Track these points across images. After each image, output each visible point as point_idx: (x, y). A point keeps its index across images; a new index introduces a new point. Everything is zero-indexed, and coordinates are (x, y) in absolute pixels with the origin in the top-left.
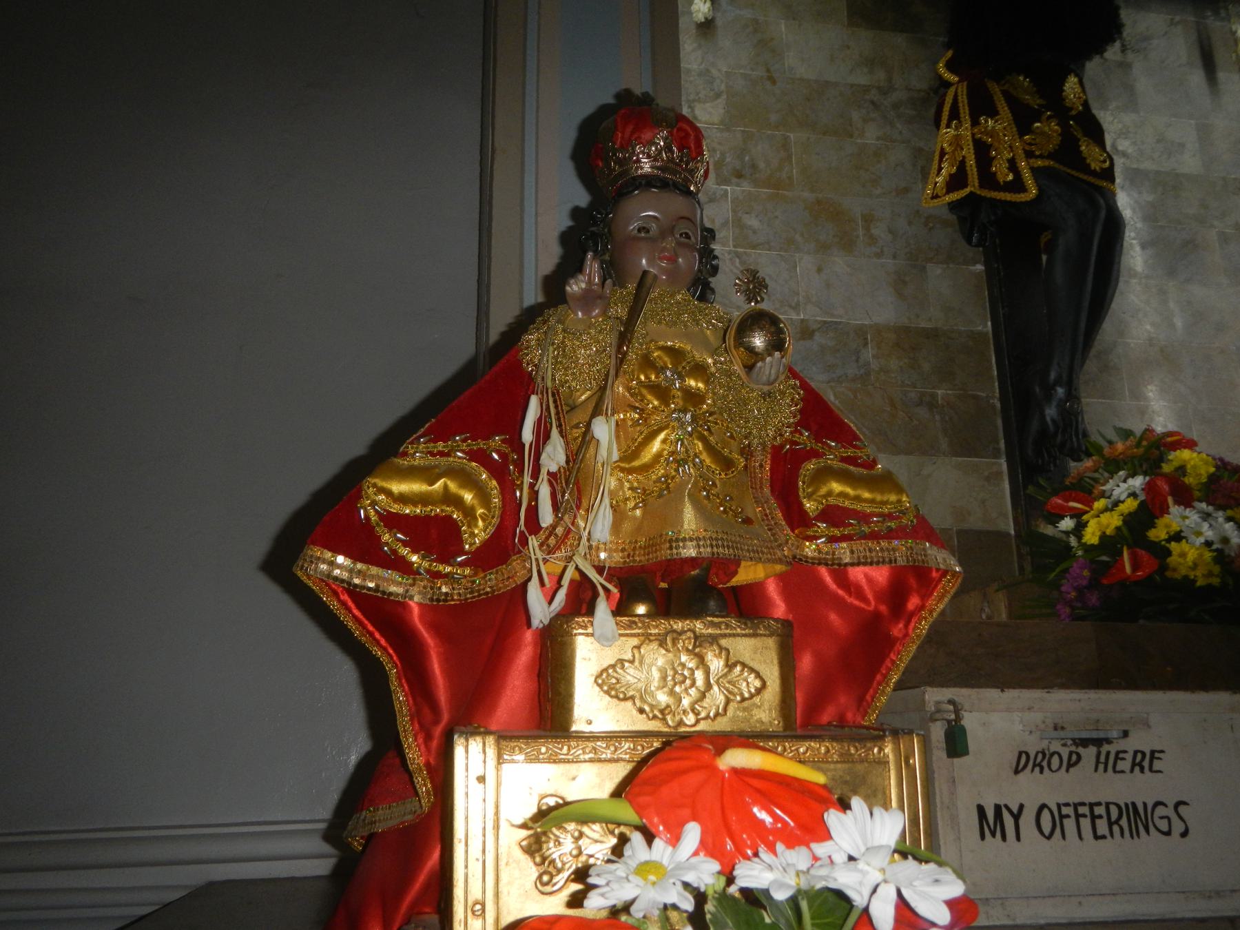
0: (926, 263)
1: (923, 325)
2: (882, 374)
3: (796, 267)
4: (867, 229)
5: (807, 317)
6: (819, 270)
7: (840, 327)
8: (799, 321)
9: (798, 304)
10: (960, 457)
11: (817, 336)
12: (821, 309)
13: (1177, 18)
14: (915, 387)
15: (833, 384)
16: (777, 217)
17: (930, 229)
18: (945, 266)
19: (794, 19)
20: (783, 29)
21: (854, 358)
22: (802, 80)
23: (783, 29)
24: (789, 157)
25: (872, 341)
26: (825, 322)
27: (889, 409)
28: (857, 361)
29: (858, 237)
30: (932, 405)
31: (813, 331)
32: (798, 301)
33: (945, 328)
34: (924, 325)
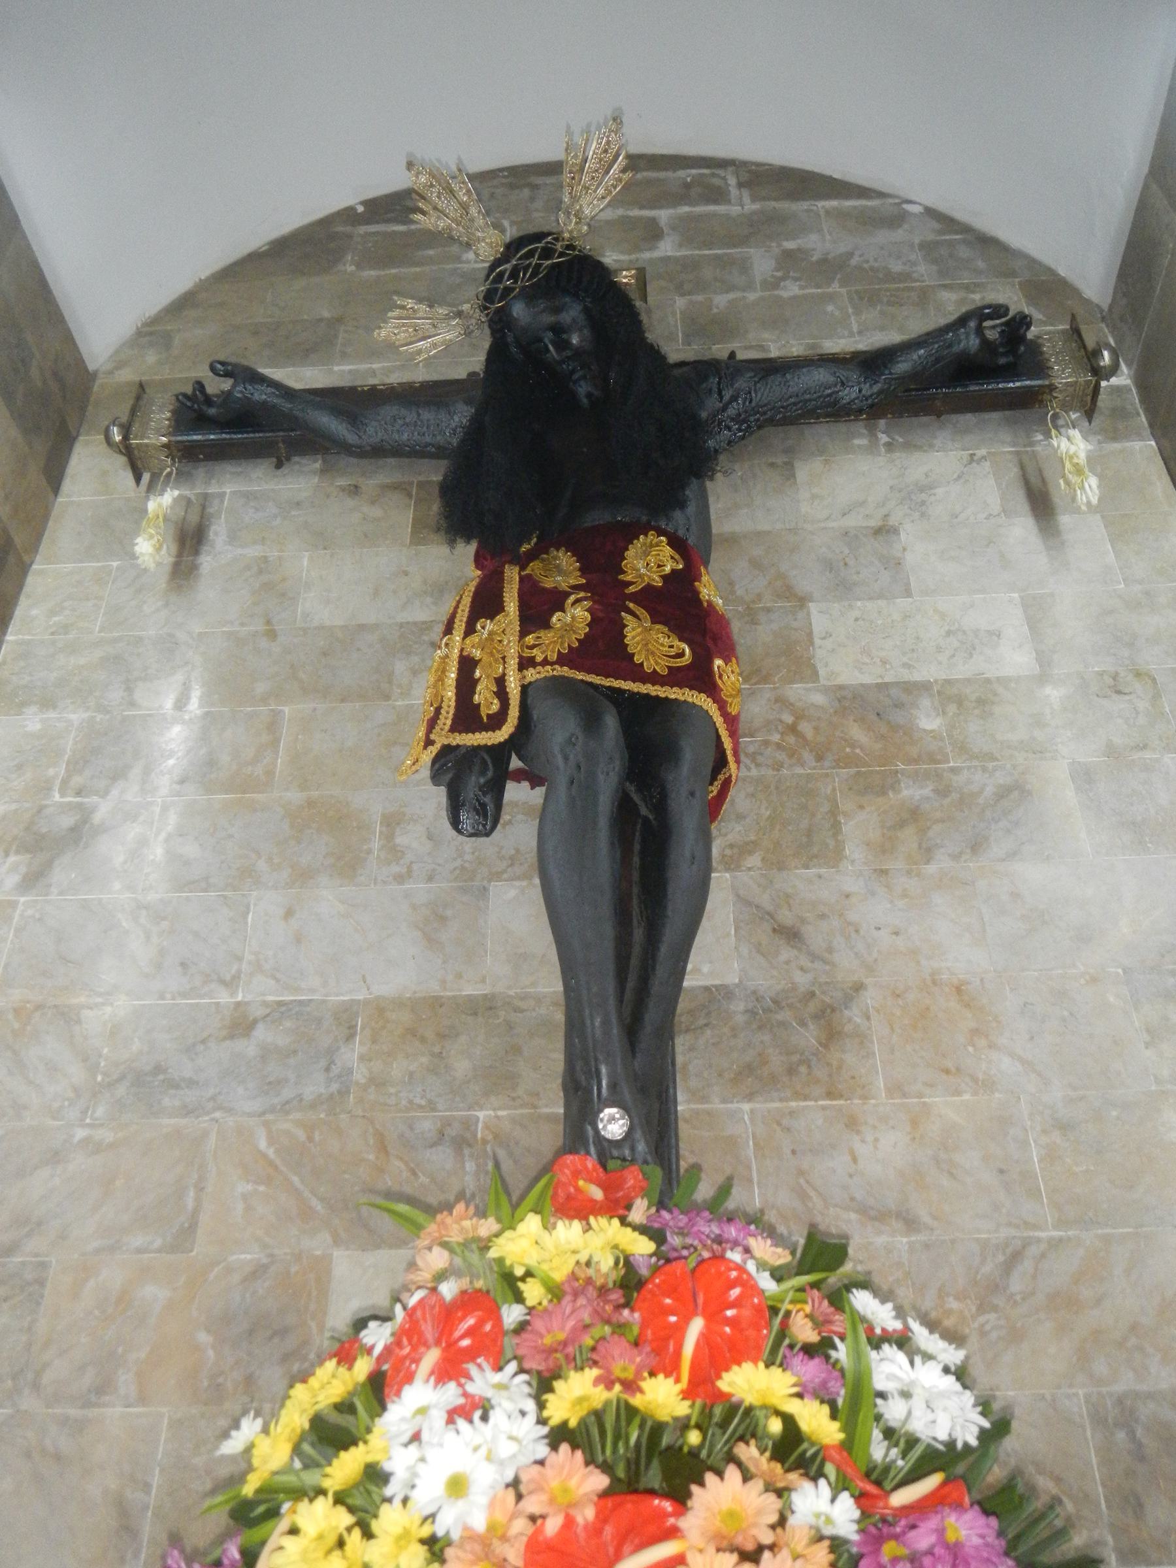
0: (490, 881)
1: (469, 990)
2: (372, 1089)
3: (248, 913)
4: (389, 837)
5: (249, 998)
6: (289, 914)
7: (308, 1009)
8: (232, 1006)
9: (237, 977)
11: (261, 1033)
12: (277, 980)
14: (434, 1110)
15: (269, 1117)
16: (231, 836)
18: (524, 883)
19: (325, 548)
20: (305, 564)
21: (323, 1063)
22: (321, 628)
23: (305, 564)
24: (275, 743)
25: (363, 1028)
26: (280, 1004)
27: (371, 1157)
28: (327, 1069)
29: (369, 852)
30: (462, 1142)
31: (255, 1022)
32: (239, 971)
33: (511, 993)
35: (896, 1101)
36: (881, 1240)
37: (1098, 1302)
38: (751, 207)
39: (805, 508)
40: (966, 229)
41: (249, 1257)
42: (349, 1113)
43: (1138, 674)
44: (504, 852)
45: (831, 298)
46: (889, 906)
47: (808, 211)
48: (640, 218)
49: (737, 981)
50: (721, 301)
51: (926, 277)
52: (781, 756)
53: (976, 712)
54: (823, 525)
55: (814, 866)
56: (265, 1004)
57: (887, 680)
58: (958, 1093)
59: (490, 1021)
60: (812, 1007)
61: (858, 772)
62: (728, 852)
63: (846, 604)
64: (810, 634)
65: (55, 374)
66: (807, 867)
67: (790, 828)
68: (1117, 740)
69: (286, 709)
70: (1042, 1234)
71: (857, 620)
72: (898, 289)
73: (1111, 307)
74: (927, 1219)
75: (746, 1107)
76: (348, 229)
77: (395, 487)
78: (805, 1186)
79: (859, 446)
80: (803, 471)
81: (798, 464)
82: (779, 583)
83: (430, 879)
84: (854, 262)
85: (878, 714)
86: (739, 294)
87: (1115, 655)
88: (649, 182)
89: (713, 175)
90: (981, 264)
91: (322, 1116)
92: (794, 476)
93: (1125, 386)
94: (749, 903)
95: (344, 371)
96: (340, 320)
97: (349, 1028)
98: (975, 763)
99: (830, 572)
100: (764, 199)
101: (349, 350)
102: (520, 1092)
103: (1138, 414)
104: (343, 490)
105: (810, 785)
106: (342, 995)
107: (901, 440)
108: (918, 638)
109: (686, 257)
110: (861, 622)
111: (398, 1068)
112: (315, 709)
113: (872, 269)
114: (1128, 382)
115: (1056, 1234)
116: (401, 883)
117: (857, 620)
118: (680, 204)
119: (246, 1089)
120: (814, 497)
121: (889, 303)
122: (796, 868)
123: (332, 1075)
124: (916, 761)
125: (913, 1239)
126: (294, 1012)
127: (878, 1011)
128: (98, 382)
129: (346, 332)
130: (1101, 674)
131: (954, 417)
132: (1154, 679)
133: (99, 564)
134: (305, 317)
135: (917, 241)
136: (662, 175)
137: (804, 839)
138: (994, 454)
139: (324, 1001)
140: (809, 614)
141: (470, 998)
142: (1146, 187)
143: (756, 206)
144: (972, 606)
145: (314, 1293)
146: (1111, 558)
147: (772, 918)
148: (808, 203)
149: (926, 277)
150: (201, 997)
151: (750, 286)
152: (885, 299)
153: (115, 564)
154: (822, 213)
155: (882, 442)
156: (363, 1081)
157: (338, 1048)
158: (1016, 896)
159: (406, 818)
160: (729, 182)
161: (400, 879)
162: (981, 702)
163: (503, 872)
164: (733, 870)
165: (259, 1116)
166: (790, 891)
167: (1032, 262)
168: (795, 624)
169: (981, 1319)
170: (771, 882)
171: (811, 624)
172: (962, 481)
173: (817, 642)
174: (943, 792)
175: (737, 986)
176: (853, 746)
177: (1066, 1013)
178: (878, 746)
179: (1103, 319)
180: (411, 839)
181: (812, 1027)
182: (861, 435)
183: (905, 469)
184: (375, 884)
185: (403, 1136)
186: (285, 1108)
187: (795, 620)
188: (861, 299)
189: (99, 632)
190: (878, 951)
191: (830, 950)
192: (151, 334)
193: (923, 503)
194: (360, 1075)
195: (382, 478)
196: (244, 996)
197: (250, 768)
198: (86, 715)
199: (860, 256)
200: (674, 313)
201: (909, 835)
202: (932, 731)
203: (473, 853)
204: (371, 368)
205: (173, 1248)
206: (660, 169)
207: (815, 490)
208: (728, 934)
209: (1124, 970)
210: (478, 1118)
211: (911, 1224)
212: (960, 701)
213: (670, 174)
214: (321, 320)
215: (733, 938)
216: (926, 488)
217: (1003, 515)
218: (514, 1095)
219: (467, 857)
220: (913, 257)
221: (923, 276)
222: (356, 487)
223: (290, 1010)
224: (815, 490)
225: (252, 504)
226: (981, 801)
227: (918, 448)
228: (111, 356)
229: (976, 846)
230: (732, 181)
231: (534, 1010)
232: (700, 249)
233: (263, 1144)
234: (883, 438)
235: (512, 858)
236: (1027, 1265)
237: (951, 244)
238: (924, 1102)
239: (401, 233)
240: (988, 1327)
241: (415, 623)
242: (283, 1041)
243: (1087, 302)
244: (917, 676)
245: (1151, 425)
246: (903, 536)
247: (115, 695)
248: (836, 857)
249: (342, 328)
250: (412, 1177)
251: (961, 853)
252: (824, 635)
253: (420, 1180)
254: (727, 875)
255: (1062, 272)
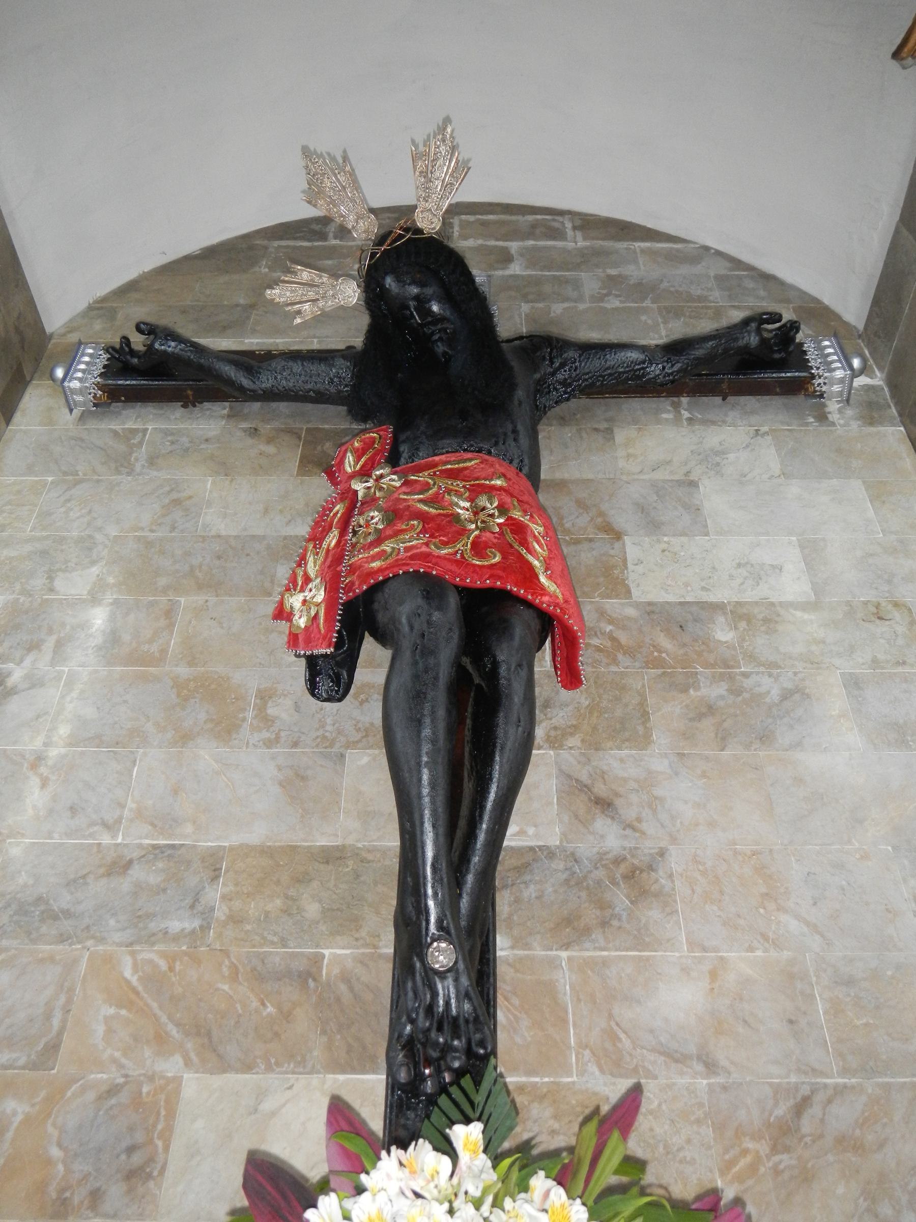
0: (347, 747)
4: (261, 709)
10: (344, 1072)
11: (137, 873)
13: (765, 429)
15: (138, 948)
16: (125, 702)
17: (362, 703)
19: (226, 475)
21: (189, 901)
24: (171, 626)
25: (227, 871)
26: (155, 847)
31: (130, 862)
33: (360, 845)
34: (323, 841)
35: (697, 954)
36: (683, 1081)
37: (881, 1146)
38: (581, 243)
39: (621, 463)
40: (750, 268)
41: (105, 1076)
42: (208, 946)
43: (896, 605)
44: (360, 725)
45: (645, 310)
46: (690, 784)
47: (626, 249)
48: (496, 247)
49: (558, 843)
50: (558, 309)
51: (719, 300)
52: (597, 656)
53: (763, 629)
54: (636, 477)
55: (626, 748)
56: (140, 846)
57: (688, 599)
58: (751, 949)
59: (340, 869)
60: (623, 868)
61: (664, 673)
62: (553, 733)
63: (655, 538)
64: (625, 561)
65: (17, 330)
66: (620, 749)
67: (606, 716)
68: (881, 657)
69: (182, 600)
70: (828, 1081)
71: (663, 551)
72: (695, 307)
73: (866, 328)
74: (724, 1062)
75: (564, 954)
76: (265, 242)
77: (290, 431)
78: (615, 1028)
79: (666, 420)
80: (620, 435)
81: (616, 430)
82: (600, 520)
83: (295, 744)
84: (665, 285)
85: (681, 627)
86: (572, 304)
87: (876, 589)
88: (502, 223)
89: (554, 220)
90: (762, 293)
91: (184, 948)
92: (613, 439)
93: (879, 386)
94: (569, 777)
95: (252, 343)
96: (252, 306)
97: (215, 870)
98: (762, 669)
99: (642, 513)
100: (593, 239)
101: (258, 328)
102: (363, 933)
103: (889, 407)
104: (245, 431)
105: (623, 681)
106: (210, 841)
107: (700, 416)
108: (714, 568)
109: (530, 276)
110: (666, 553)
111: (253, 909)
112: (207, 601)
113: (677, 291)
114: (881, 383)
115: (840, 1080)
116: (268, 748)
117: (663, 551)
118: (528, 239)
119: (118, 922)
120: (629, 456)
121: (690, 317)
122: (611, 749)
123: (195, 912)
124: (713, 666)
125: (712, 1081)
126: (166, 854)
127: (681, 875)
128: (53, 341)
129: (257, 315)
130: (866, 603)
131: (743, 399)
132: (910, 610)
133: (36, 479)
134: (226, 303)
135: (712, 274)
136: (514, 218)
137: (618, 726)
138: (775, 430)
139: (194, 846)
140: (624, 544)
141: (323, 849)
142: (897, 232)
143: (587, 243)
144: (758, 545)
145: (163, 1113)
146: (871, 513)
147: (590, 790)
148: (628, 243)
149: (719, 300)
150: (84, 837)
151: (580, 299)
152: (688, 314)
153: (50, 479)
154: (638, 250)
155: (685, 417)
156: (223, 918)
157: (204, 888)
158: (799, 781)
159: (278, 693)
160: (566, 226)
161: (269, 744)
162: (766, 621)
163: (359, 741)
164: (556, 748)
165: (127, 946)
166: (605, 768)
167: (803, 294)
168: (612, 552)
169: (776, 1158)
170: (589, 760)
171: (625, 553)
172: (749, 449)
173: (630, 565)
174: (736, 691)
175: (558, 847)
176: (660, 652)
177: (844, 883)
178: (681, 652)
179: (860, 336)
180: (280, 710)
181: (623, 886)
182: (669, 411)
183: (703, 438)
184: (247, 747)
185: (255, 969)
186: (150, 939)
187: (613, 548)
188: (669, 312)
189: (30, 531)
190: (681, 823)
191: (639, 820)
192: (98, 309)
193: (718, 464)
194: (221, 913)
195: (276, 424)
196: (123, 839)
197: (147, 646)
198: (12, 597)
199: (668, 282)
200: (520, 315)
201: (707, 724)
202: (726, 642)
203: (334, 725)
204: (275, 342)
205: (34, 1066)
206: (512, 214)
207: (631, 451)
208: (552, 803)
209: (893, 848)
210: (323, 956)
211: (711, 1067)
212: (748, 618)
213: (520, 218)
214: (237, 305)
215: (556, 807)
216: (724, 453)
217: (782, 476)
218: (357, 936)
219: (329, 728)
220: (710, 285)
221: (716, 298)
222: (256, 429)
223: (163, 852)
224: (631, 451)
225: (169, 438)
226: (768, 700)
227: (714, 423)
228: (66, 324)
229: (765, 738)
230: (569, 225)
231: (379, 861)
232: (542, 270)
233: (128, 973)
234: (686, 414)
235: (366, 730)
236: (815, 1110)
237: (739, 278)
238: (722, 958)
239: (306, 247)
240: (781, 1167)
241: (297, 536)
242: (154, 879)
243: (846, 324)
244: (712, 598)
245: (900, 415)
246: (701, 488)
247: (39, 582)
248: (645, 741)
249: (254, 312)
250: (262, 1007)
251: (751, 742)
252: (636, 562)
253: (269, 1010)
254: (552, 752)
255: (826, 301)
